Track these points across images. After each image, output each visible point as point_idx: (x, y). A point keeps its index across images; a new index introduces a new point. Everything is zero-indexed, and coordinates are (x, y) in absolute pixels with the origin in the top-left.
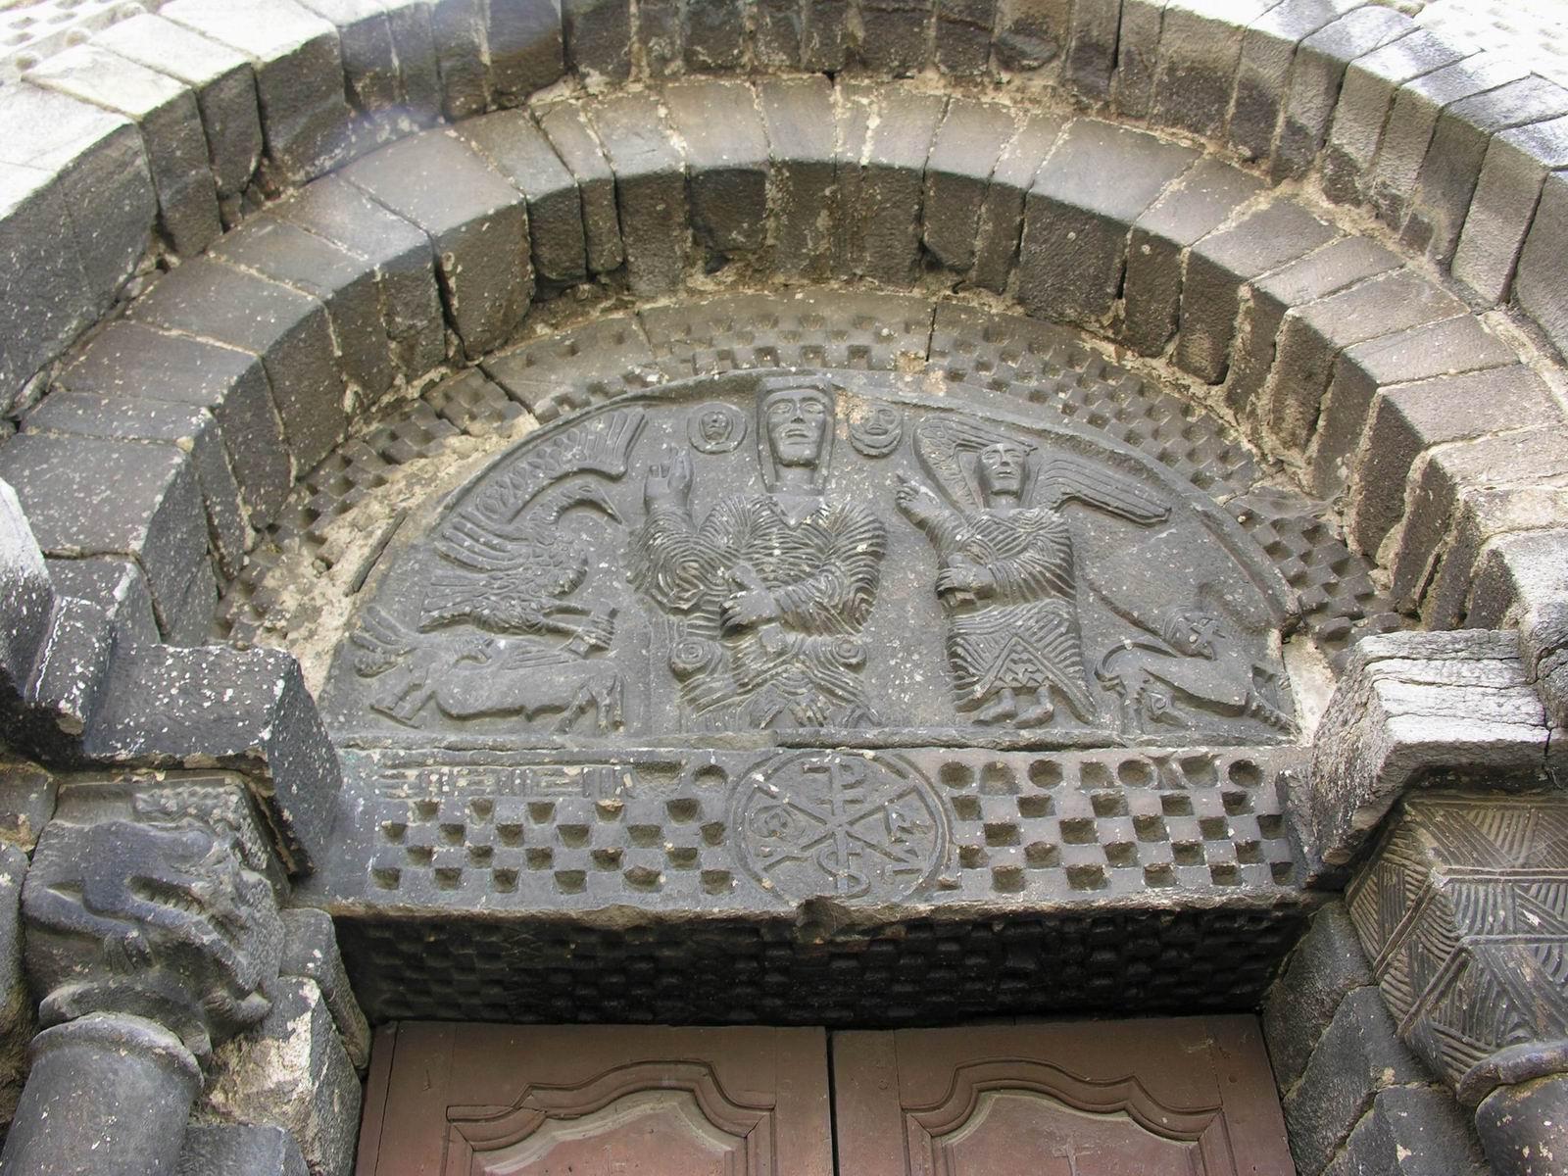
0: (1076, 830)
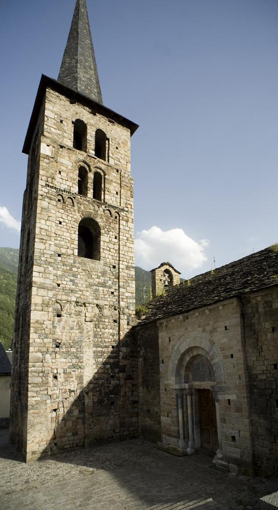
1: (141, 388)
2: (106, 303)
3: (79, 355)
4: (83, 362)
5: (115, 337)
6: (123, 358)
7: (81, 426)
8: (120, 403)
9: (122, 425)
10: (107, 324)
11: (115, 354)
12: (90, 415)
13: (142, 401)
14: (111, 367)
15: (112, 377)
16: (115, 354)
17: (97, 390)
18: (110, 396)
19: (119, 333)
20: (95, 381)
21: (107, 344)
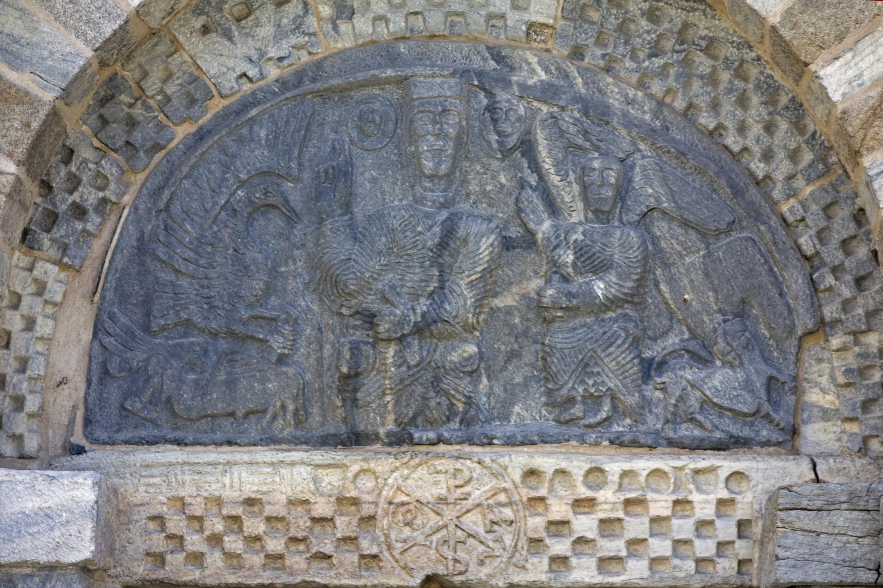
0: (608, 526)
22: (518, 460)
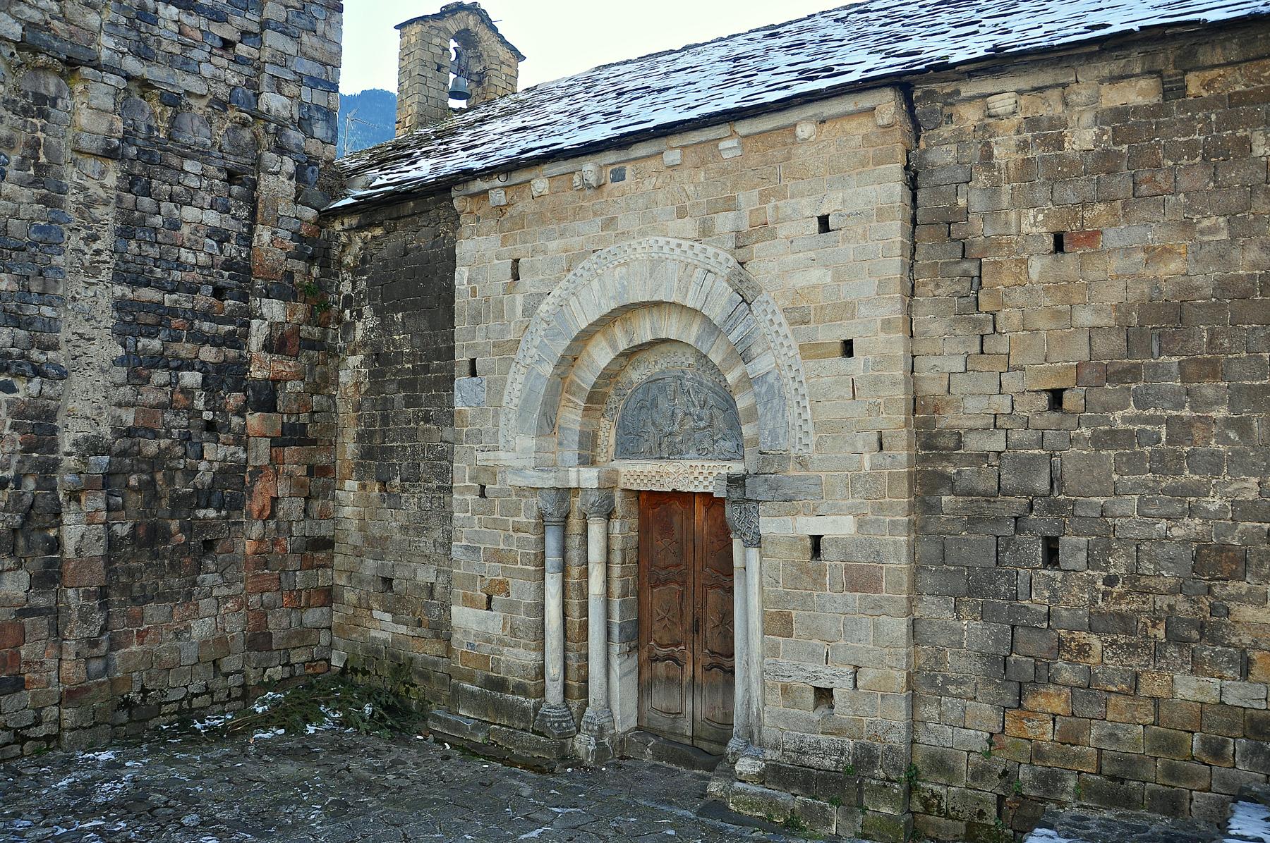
1: (352, 484)
2: (190, 83)
3: (31, 311)
4: (55, 347)
5: (231, 249)
6: (267, 347)
7: (39, 647)
8: (249, 547)
9: (259, 640)
10: (195, 183)
11: (231, 328)
12: (88, 595)
13: (355, 538)
14: (205, 384)
15: (210, 427)
16: (231, 328)
17: (133, 481)
18: (201, 513)
19: (246, 239)
20: (119, 444)
21: (188, 277)
22: (688, 463)
